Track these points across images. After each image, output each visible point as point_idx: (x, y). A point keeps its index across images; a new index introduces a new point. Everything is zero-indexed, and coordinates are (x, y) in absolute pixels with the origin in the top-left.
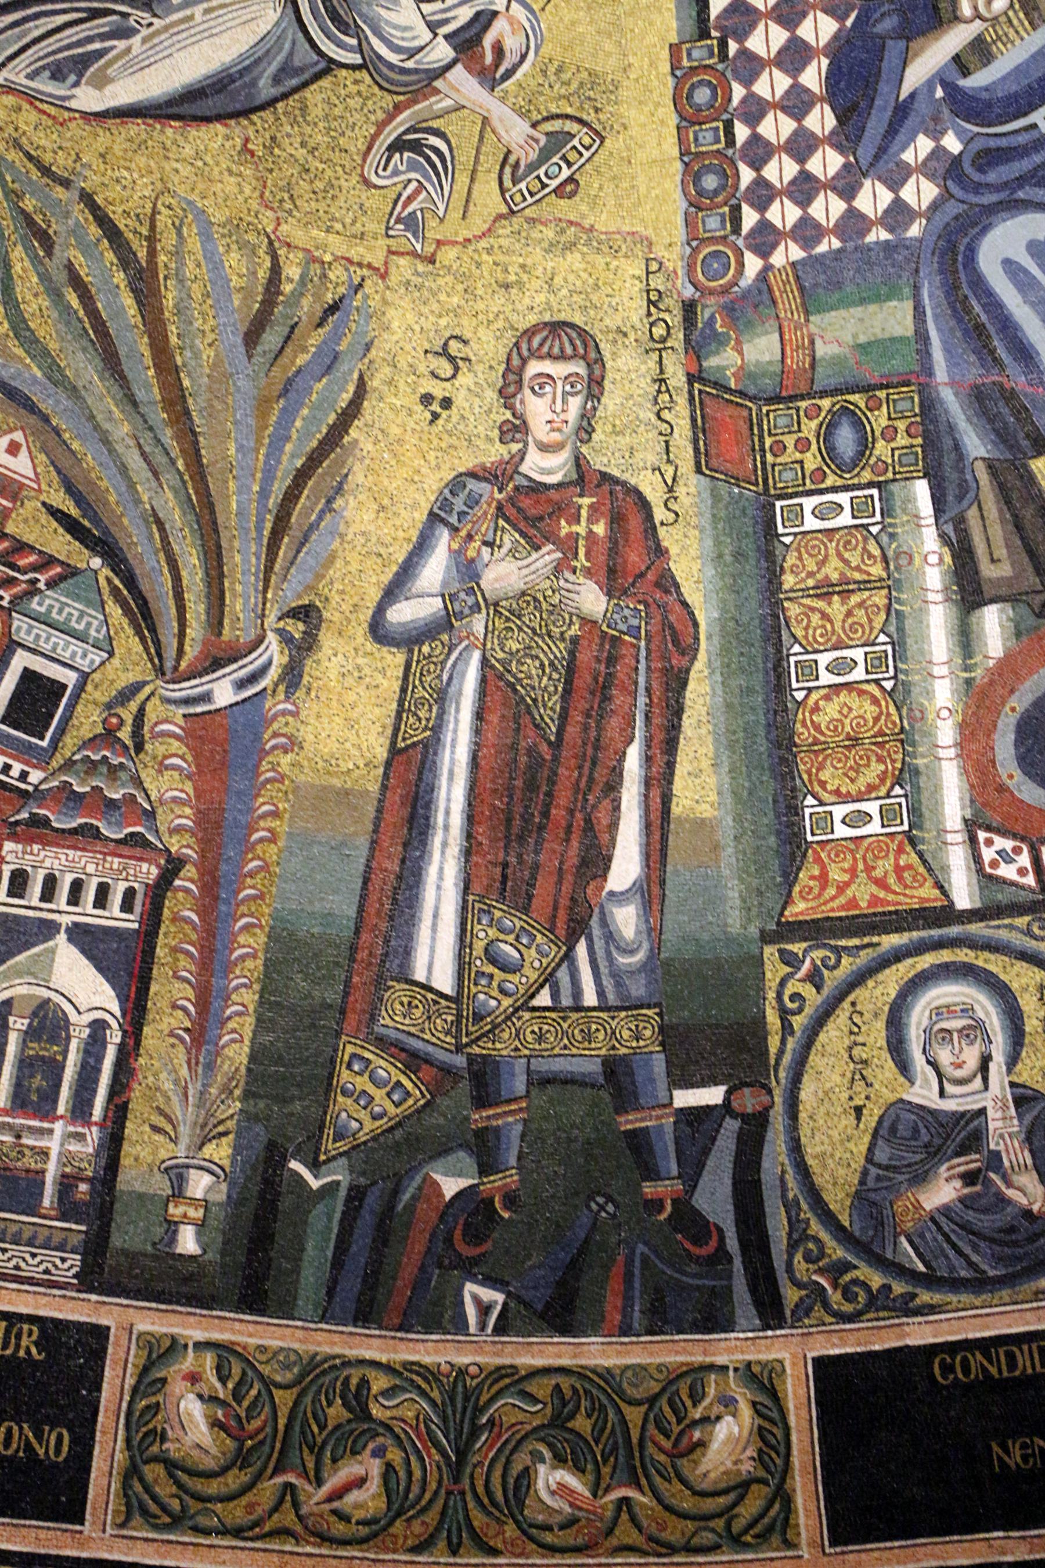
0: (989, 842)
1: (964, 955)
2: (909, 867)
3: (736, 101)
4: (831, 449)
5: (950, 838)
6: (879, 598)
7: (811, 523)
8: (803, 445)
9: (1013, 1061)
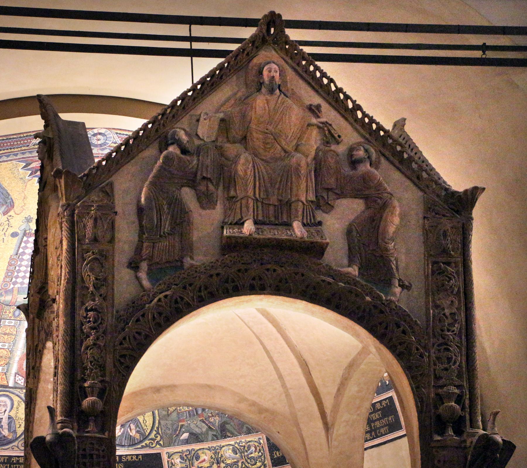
0: (18, 377)
1: (7, 393)
2: (4, 378)
3: (18, 264)
4: (14, 314)
5: (12, 375)
6: (13, 337)
7: (7, 324)
8: (10, 313)
9: (10, 411)
